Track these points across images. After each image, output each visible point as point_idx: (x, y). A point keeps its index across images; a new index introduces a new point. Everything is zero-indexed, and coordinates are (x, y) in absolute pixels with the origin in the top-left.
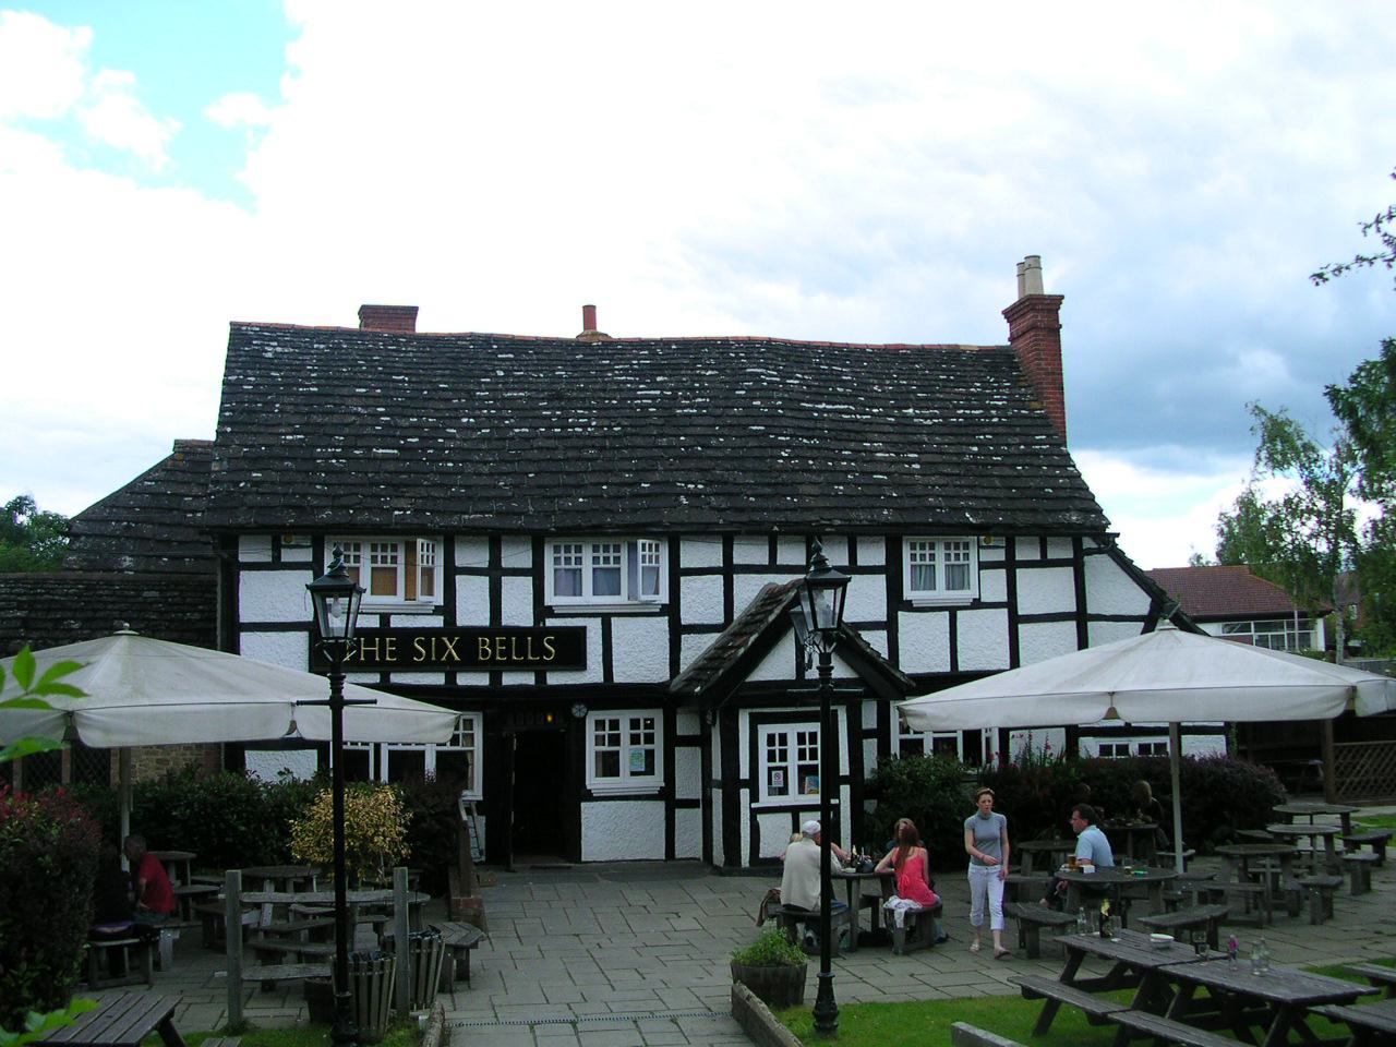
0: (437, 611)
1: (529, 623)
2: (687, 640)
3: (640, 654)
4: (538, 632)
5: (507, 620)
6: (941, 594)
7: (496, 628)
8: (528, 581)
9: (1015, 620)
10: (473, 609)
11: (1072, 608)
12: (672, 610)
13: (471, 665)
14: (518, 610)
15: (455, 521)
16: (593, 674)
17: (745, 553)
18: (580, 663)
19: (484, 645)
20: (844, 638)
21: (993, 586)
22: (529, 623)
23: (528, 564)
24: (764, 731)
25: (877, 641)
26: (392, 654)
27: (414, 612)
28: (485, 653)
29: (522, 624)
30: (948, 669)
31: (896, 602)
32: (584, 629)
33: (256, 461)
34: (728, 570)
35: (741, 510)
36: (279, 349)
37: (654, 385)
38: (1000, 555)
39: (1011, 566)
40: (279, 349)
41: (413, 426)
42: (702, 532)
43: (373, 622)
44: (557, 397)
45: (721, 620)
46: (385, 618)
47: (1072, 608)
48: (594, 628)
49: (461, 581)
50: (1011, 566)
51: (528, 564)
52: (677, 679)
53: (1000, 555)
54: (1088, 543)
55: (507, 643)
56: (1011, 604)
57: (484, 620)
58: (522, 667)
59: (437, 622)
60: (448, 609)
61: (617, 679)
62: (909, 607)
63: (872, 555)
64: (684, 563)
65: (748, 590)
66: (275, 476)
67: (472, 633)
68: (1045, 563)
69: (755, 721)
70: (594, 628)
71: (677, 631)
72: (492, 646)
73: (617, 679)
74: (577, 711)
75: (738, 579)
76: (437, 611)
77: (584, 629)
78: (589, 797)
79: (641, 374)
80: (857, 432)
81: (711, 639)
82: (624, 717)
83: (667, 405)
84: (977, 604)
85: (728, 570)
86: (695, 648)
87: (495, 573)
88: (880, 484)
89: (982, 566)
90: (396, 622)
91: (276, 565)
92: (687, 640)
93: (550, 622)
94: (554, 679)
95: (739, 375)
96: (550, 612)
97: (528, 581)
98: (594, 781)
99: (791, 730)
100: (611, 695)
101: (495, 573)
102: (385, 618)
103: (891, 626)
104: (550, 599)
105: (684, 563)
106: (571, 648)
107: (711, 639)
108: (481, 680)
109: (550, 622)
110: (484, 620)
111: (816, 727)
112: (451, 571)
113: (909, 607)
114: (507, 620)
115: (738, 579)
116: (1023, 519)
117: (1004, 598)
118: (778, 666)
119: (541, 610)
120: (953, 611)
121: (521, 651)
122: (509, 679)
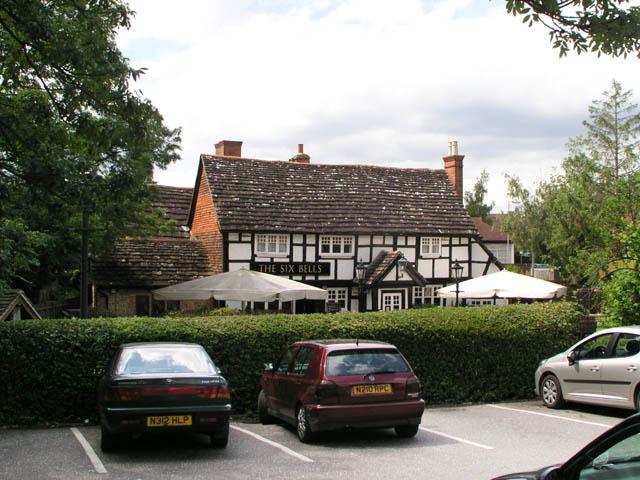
4: (316, 264)
5: (308, 260)
6: (431, 254)
7: (304, 262)
10: (298, 257)
11: (467, 259)
15: (294, 230)
16: (332, 277)
17: (378, 240)
18: (328, 274)
19: (301, 267)
21: (445, 252)
23: (314, 242)
24: (385, 295)
27: (281, 256)
31: (418, 256)
34: (372, 246)
35: (376, 228)
37: (340, 182)
38: (448, 243)
39: (450, 246)
42: (365, 234)
46: (272, 259)
47: (467, 259)
48: (332, 262)
49: (294, 247)
50: (450, 246)
51: (314, 242)
53: (448, 243)
54: (473, 240)
57: (301, 260)
58: (312, 274)
59: (288, 260)
60: (290, 256)
62: (421, 258)
64: (360, 244)
65: (377, 252)
66: (236, 213)
67: (297, 264)
68: (460, 245)
69: (383, 292)
70: (332, 262)
75: (374, 249)
79: (336, 178)
80: (403, 201)
83: (346, 190)
84: (441, 258)
85: (372, 246)
87: (304, 245)
88: (413, 219)
89: (443, 246)
90: (275, 260)
91: (240, 242)
95: (366, 180)
96: (320, 258)
99: (392, 295)
101: (304, 245)
102: (272, 259)
104: (320, 254)
105: (360, 244)
110: (301, 260)
111: (400, 295)
112: (292, 245)
113: (421, 258)
114: (308, 260)
115: (374, 249)
116: (455, 232)
117: (448, 255)
118: (391, 277)
119: (318, 257)
120: (434, 259)
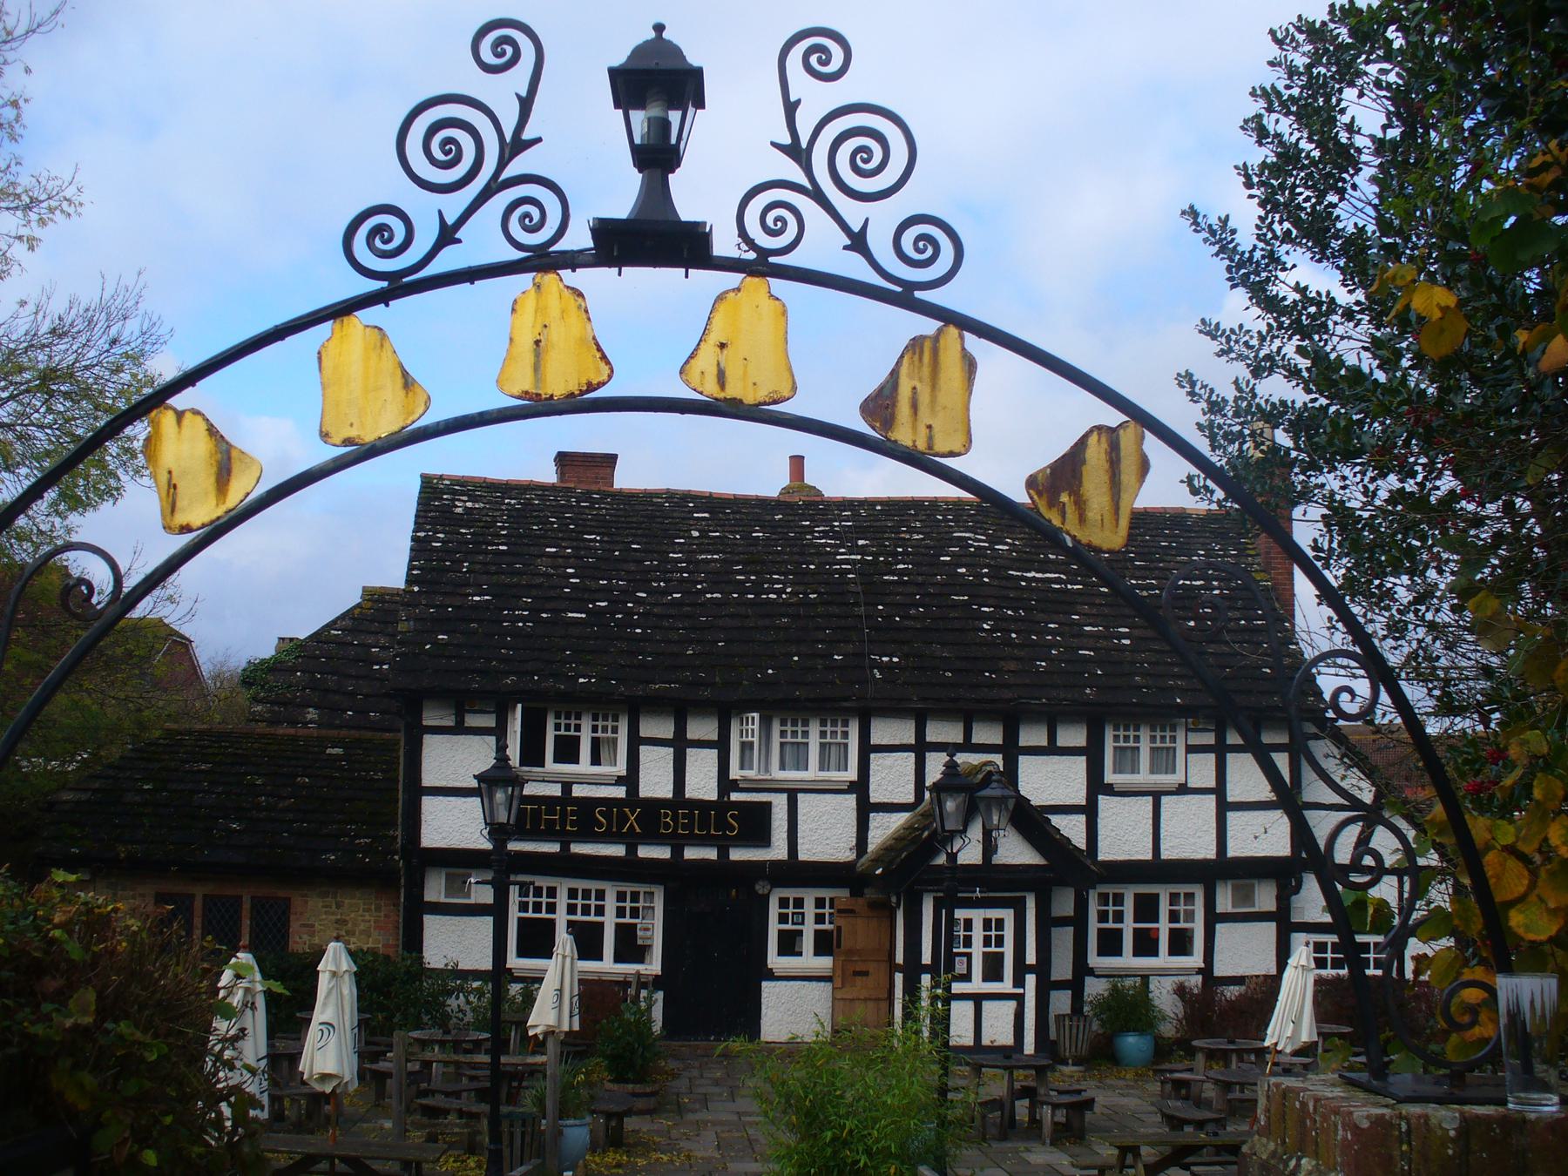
0: (619, 781)
1: (714, 796)
2: (876, 820)
3: (826, 831)
4: (722, 805)
6: (1144, 777)
8: (713, 754)
9: (1224, 807)
10: (656, 782)
12: (860, 787)
13: (654, 839)
14: (702, 782)
16: (778, 850)
17: (939, 732)
18: (764, 840)
20: (1032, 822)
21: (1202, 771)
22: (714, 796)
25: (1073, 829)
26: (573, 824)
28: (667, 826)
29: (706, 798)
30: (1149, 856)
31: (1097, 785)
32: (768, 805)
33: (441, 623)
36: (469, 504)
39: (1221, 751)
40: (469, 504)
41: (603, 589)
42: (894, 711)
43: (555, 790)
44: (751, 563)
45: (911, 799)
46: (567, 787)
48: (779, 802)
49: (645, 752)
50: (1221, 751)
52: (863, 860)
55: (690, 816)
56: (1220, 790)
59: (620, 792)
60: (631, 779)
61: (802, 856)
62: (1110, 790)
63: (1073, 736)
64: (876, 739)
67: (655, 804)
70: (779, 802)
71: (865, 809)
72: (675, 818)
73: (802, 856)
74: (761, 888)
76: (619, 781)
77: (768, 805)
78: (771, 976)
81: (899, 820)
82: (810, 896)
84: (1183, 789)
85: (921, 748)
86: (884, 828)
87: (680, 745)
89: (1191, 749)
90: (578, 791)
91: (459, 729)
92: (876, 820)
93: (734, 797)
94: (736, 855)
96: (735, 786)
97: (713, 754)
98: (775, 961)
100: (796, 872)
101: (680, 745)
102: (567, 787)
103: (1090, 810)
105: (876, 739)
106: (755, 824)
107: (899, 820)
108: (662, 853)
109: (734, 797)
111: (1008, 915)
112: (635, 742)
119: (726, 784)
120: (1157, 796)
121: (704, 824)
122: (691, 853)
